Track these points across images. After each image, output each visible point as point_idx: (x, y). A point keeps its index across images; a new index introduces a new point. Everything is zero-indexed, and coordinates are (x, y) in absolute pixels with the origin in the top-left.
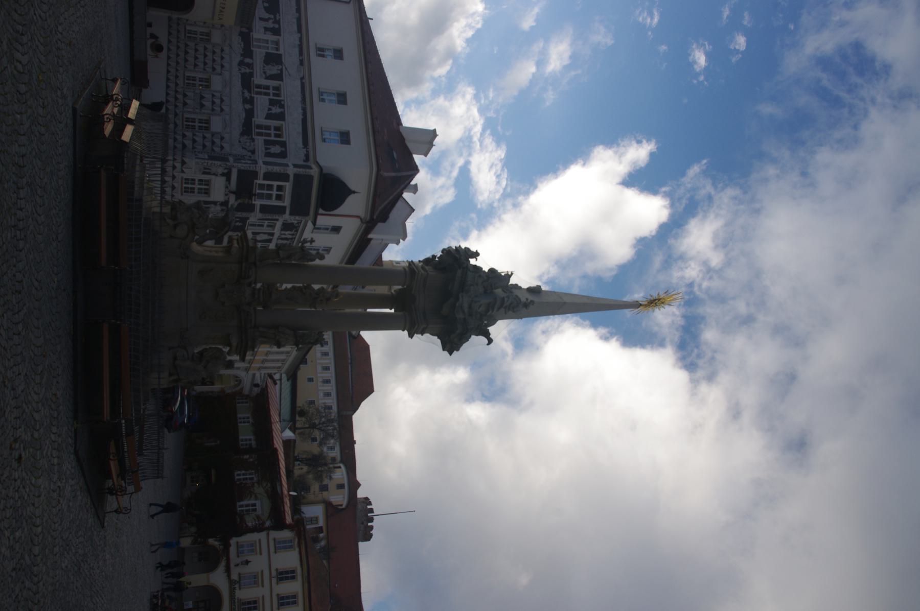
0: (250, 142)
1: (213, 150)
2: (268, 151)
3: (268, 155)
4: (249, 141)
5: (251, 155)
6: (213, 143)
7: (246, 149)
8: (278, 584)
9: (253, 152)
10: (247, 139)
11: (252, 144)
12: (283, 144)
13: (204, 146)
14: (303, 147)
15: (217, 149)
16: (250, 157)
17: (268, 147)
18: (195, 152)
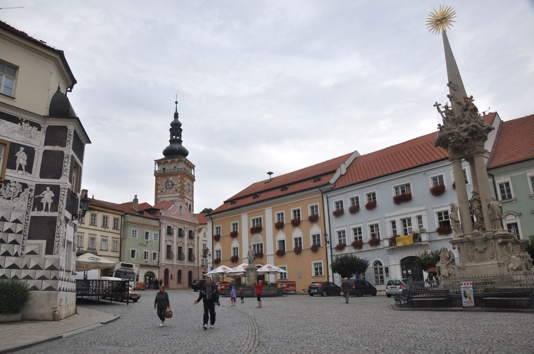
0: (10, 186)
1: (20, 233)
2: (24, 168)
3: (29, 168)
4: (8, 188)
5: (29, 189)
6: (9, 231)
7: (20, 193)
8: (84, 224)
9: (25, 186)
10: (5, 189)
11: (11, 184)
12: (14, 147)
13: (14, 242)
14: (19, 124)
15: (19, 227)
16: (31, 190)
17: (18, 166)
18: (22, 254)
